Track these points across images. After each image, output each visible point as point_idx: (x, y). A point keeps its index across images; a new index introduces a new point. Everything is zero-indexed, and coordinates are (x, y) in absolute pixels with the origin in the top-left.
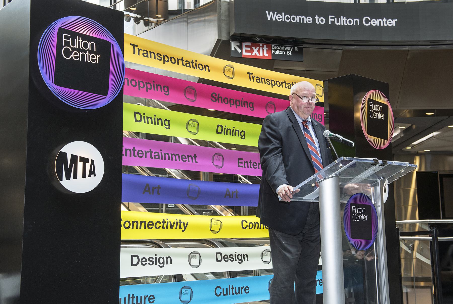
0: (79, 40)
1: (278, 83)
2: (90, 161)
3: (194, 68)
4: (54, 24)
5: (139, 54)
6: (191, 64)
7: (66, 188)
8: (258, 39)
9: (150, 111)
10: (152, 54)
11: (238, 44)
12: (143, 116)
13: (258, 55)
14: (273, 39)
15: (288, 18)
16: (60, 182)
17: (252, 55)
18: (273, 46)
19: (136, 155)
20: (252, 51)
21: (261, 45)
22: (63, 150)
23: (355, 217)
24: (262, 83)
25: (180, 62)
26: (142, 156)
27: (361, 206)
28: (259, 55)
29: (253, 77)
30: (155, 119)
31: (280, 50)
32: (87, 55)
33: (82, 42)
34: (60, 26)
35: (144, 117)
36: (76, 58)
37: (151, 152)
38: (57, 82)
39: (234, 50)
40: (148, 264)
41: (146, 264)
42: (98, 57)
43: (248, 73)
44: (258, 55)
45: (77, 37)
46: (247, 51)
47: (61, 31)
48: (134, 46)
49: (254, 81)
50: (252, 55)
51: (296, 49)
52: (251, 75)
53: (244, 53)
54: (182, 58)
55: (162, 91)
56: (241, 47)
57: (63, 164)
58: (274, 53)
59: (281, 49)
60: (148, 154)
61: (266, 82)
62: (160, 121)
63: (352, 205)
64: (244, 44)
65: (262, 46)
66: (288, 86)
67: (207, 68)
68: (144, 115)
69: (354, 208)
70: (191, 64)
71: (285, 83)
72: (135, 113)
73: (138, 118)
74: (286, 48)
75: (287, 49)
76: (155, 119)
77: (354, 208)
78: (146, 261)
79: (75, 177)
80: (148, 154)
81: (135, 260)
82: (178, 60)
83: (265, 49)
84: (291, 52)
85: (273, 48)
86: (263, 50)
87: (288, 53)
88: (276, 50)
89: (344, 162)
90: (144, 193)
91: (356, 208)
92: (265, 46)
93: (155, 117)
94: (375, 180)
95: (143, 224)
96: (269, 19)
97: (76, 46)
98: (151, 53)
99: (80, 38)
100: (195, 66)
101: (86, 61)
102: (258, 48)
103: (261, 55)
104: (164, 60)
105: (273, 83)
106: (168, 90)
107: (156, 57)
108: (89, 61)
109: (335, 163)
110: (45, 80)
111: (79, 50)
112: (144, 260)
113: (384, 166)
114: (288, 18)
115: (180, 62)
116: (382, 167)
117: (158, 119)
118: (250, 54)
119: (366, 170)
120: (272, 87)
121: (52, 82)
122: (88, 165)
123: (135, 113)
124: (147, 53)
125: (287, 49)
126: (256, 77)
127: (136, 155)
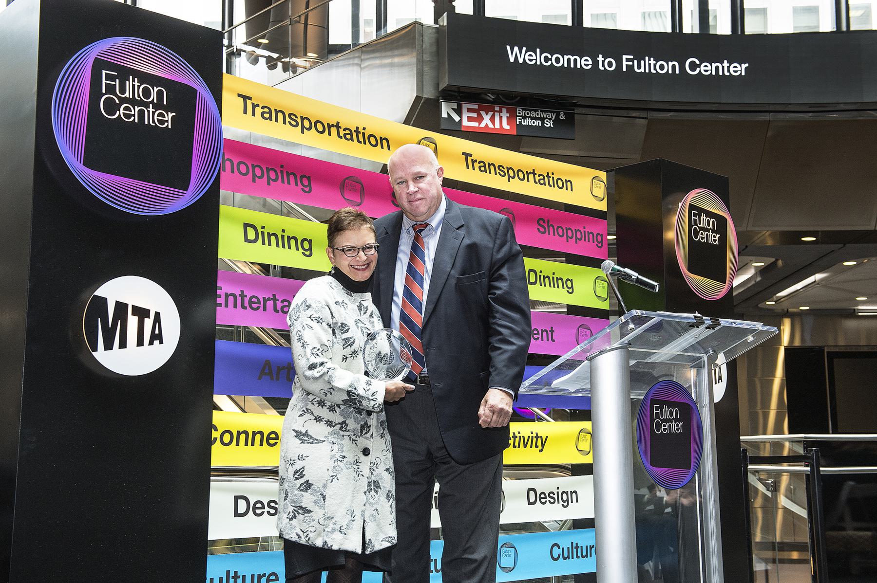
0: (134, 83)
1: (521, 174)
2: (152, 315)
3: (360, 142)
4: (86, 50)
5: (253, 114)
6: (354, 134)
7: (100, 362)
8: (491, 97)
9: (274, 222)
10: (280, 115)
11: (455, 106)
12: (260, 230)
13: (491, 125)
14: (519, 98)
15: (547, 59)
16: (92, 354)
17: (480, 126)
18: (519, 110)
19: (246, 304)
20: (480, 119)
21: (497, 108)
22: (100, 292)
23: (659, 426)
24: (490, 173)
25: (334, 130)
26: (258, 308)
27: (671, 405)
28: (493, 127)
29: (473, 162)
30: (283, 236)
31: (532, 118)
32: (149, 112)
33: (139, 87)
34: (97, 55)
35: (263, 233)
36: (128, 116)
37: (275, 300)
38: (90, 162)
39: (447, 117)
40: (266, 513)
41: (263, 512)
42: (170, 115)
43: (464, 154)
44: (491, 125)
45: (131, 77)
46: (470, 119)
47: (99, 65)
48: (245, 98)
49: (474, 169)
50: (481, 126)
51: (562, 117)
52: (470, 158)
53: (465, 123)
54: (338, 123)
55: (297, 185)
56: (459, 112)
57: (99, 319)
58: (520, 122)
59: (534, 116)
60: (270, 304)
61: (498, 171)
62: (293, 242)
63: (653, 402)
64: (465, 106)
65: (498, 110)
66: (540, 180)
67: (384, 142)
68: (263, 230)
69: (657, 409)
70: (355, 134)
71: (534, 173)
72: (246, 225)
73: (251, 235)
74: (544, 115)
75: (545, 117)
76: (283, 236)
77: (657, 409)
78: (263, 507)
79: (123, 345)
80: (270, 304)
81: (242, 504)
82: (330, 126)
83: (505, 115)
84: (552, 122)
85: (520, 113)
86: (501, 118)
87: (547, 124)
88: (524, 118)
89: (638, 320)
90: (260, 378)
91: (662, 408)
92: (504, 110)
93: (283, 234)
94: (698, 355)
95: (258, 437)
96: (512, 60)
97: (127, 95)
98: (277, 112)
99: (136, 79)
100: (361, 139)
101: (146, 123)
102: (491, 114)
103: (497, 126)
104: (303, 127)
105: (512, 174)
106: (309, 185)
107: (288, 119)
108: (153, 123)
109: (621, 323)
110: (66, 158)
111: (133, 102)
112: (259, 505)
113: (714, 329)
114: (547, 59)
115: (334, 130)
116: (712, 331)
117: (289, 238)
118: (476, 124)
119: (681, 335)
120: (509, 181)
121: (80, 163)
122: (148, 323)
123: (246, 225)
124: (270, 112)
125: (545, 117)
126: (478, 162)
127: (246, 304)
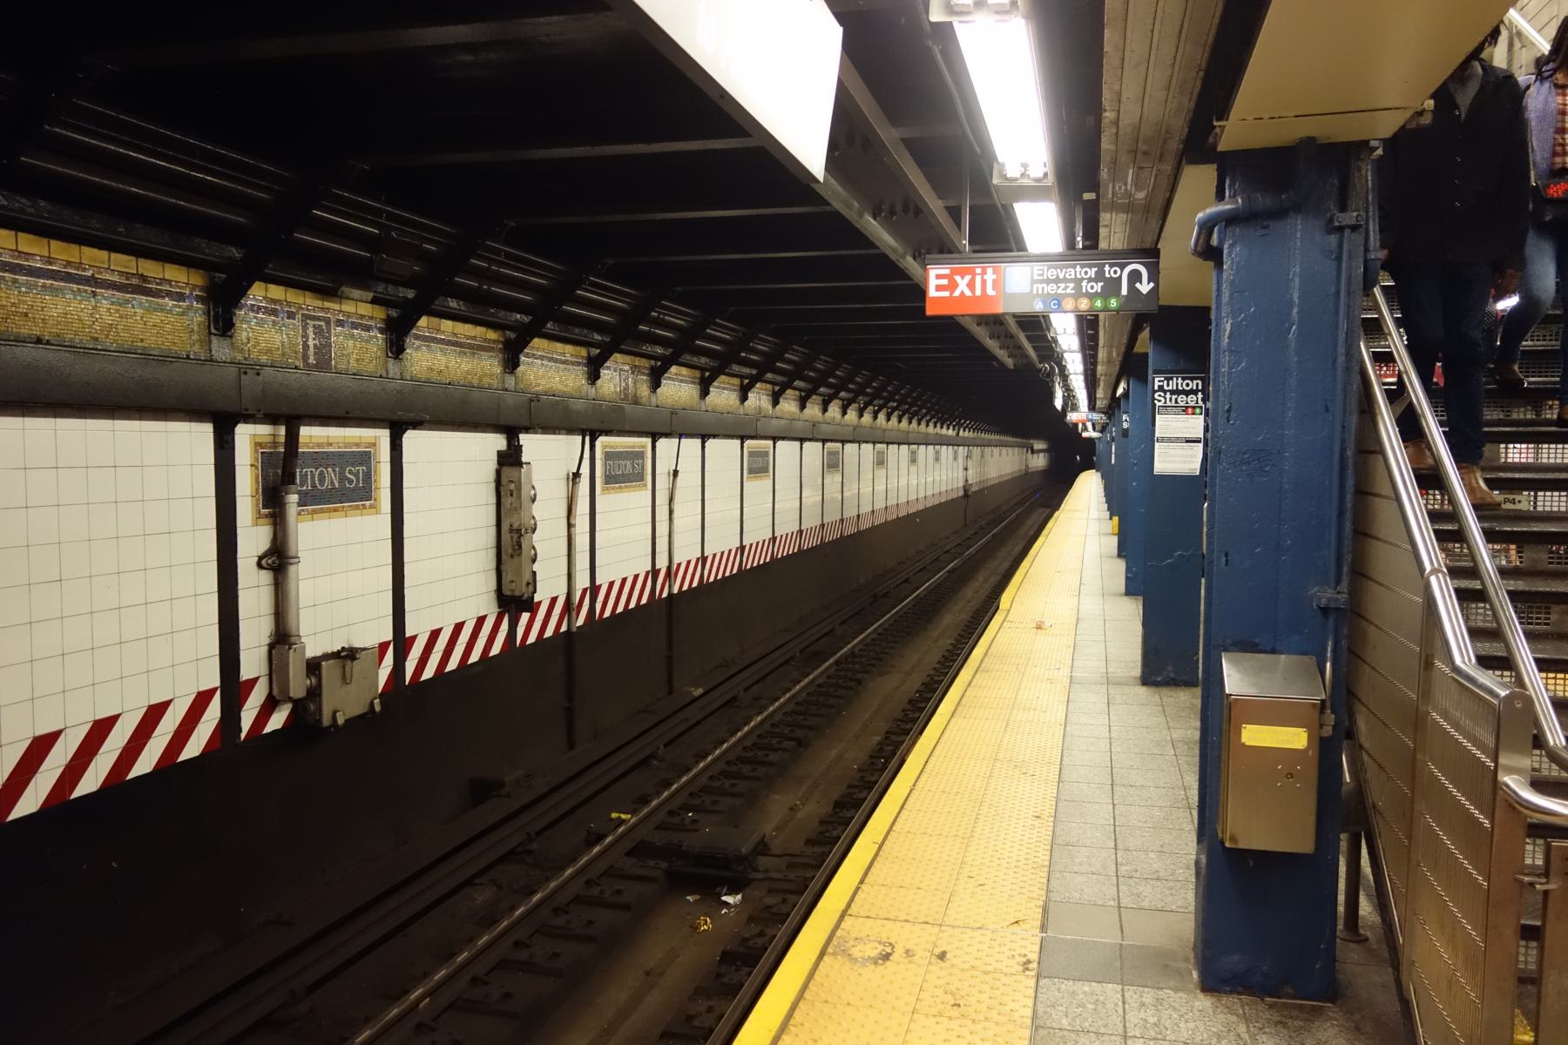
20: (953, 286)
44: (968, 293)
46: (939, 288)
102: (968, 278)
118: (946, 294)
